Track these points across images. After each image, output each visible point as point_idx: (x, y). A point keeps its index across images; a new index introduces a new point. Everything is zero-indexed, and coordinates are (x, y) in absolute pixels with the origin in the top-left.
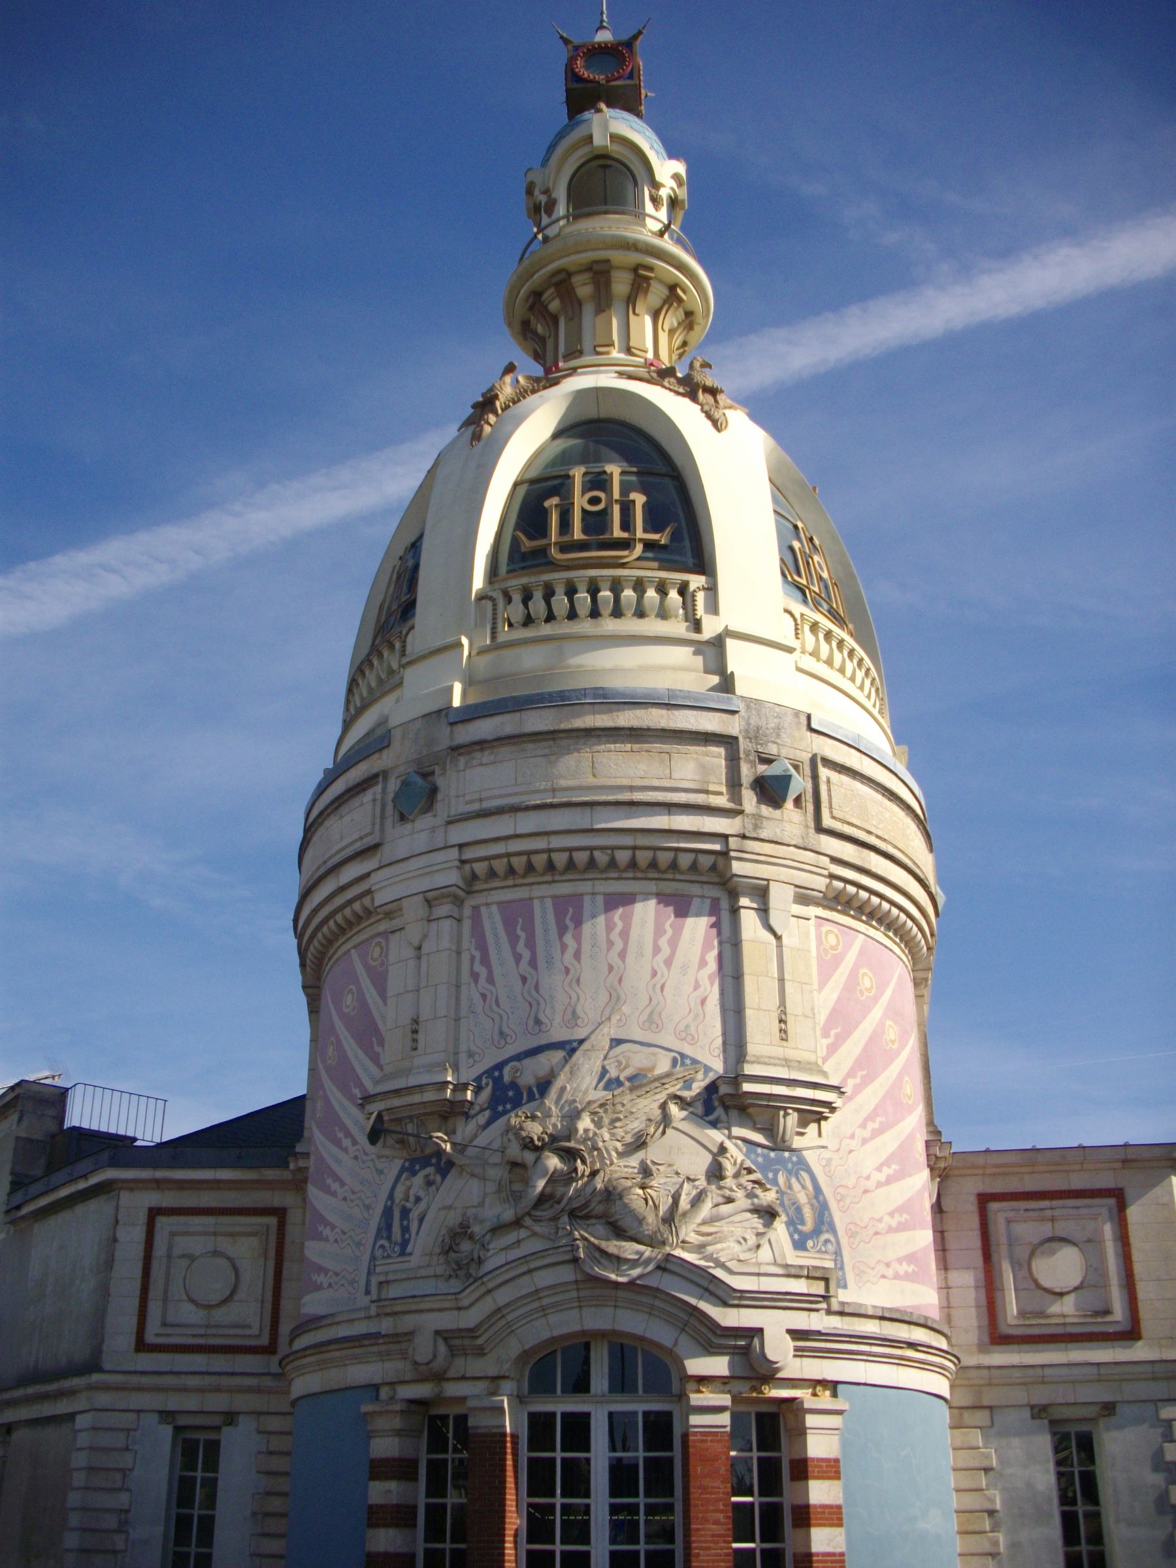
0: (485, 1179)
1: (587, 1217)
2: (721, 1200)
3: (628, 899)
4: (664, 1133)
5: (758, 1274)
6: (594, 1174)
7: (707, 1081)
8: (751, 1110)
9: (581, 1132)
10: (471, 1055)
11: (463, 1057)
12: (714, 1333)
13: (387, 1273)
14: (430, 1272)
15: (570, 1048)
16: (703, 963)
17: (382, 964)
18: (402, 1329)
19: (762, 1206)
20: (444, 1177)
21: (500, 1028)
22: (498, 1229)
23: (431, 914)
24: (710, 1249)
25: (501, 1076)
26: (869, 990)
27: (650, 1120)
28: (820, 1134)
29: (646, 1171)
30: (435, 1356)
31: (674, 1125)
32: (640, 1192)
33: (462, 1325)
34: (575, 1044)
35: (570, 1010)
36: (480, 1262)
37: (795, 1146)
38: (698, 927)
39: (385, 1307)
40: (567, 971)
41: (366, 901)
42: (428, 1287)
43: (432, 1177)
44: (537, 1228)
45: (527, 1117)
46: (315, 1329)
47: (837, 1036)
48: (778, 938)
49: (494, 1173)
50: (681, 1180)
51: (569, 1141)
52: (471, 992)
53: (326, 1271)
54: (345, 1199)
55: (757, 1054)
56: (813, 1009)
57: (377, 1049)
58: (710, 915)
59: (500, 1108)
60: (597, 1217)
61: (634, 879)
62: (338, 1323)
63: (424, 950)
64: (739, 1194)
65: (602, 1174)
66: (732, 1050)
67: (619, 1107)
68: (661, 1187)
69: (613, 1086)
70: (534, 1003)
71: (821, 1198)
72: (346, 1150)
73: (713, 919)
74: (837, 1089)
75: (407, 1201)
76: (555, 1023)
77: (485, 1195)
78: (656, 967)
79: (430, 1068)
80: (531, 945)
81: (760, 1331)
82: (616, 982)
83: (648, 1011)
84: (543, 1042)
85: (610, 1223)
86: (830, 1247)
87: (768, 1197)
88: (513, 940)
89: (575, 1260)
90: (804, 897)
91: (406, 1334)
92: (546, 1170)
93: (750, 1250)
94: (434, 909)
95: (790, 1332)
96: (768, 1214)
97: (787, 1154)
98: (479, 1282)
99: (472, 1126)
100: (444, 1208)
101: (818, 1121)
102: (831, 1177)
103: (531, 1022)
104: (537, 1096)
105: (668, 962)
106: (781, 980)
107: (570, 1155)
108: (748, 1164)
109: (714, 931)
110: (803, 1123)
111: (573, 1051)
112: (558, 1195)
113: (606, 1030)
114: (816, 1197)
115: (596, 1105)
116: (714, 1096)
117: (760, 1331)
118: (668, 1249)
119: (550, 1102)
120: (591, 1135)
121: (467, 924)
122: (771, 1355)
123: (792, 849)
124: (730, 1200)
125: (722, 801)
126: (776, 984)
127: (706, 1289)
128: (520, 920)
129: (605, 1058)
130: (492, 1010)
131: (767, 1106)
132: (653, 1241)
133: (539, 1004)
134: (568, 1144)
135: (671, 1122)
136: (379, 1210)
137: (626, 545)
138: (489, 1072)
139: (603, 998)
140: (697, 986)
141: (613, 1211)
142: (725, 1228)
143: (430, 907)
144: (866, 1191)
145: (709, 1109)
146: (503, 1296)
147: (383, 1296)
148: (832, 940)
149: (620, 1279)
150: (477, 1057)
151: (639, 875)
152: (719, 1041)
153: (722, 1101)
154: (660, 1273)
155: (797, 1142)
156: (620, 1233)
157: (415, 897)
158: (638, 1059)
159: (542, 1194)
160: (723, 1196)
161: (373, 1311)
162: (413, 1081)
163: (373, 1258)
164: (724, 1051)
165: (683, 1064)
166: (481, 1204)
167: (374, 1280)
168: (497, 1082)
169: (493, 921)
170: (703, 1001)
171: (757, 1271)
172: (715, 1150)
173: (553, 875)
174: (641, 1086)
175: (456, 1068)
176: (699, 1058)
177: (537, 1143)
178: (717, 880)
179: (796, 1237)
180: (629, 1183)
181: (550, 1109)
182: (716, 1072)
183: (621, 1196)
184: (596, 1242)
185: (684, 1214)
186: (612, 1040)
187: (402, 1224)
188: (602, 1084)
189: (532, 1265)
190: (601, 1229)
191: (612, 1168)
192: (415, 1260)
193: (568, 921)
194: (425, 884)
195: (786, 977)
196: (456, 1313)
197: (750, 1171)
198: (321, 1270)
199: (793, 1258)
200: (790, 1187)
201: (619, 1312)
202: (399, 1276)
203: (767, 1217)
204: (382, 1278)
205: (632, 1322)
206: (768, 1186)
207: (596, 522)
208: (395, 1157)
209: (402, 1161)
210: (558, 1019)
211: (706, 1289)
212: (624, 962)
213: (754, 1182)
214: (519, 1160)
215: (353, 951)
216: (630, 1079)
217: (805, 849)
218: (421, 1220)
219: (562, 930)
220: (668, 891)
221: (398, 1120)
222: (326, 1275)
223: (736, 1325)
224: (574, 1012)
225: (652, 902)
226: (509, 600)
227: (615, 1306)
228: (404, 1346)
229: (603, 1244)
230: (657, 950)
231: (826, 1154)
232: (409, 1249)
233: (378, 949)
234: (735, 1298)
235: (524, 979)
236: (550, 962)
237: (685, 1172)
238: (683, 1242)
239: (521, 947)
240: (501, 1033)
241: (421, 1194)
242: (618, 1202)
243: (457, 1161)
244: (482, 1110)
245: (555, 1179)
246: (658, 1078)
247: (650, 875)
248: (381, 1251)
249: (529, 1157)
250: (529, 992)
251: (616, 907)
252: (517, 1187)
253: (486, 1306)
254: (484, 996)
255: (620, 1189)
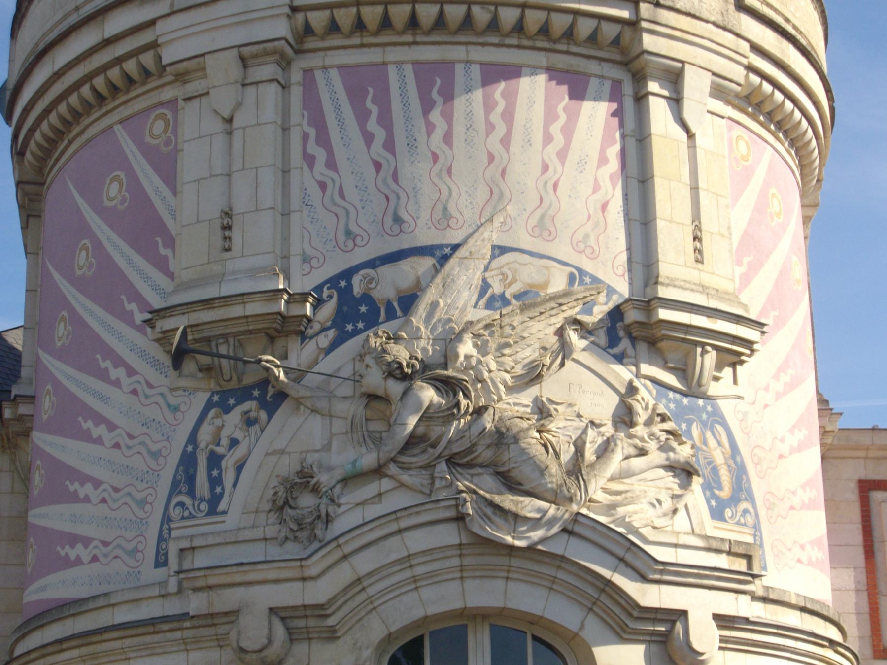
0: (331, 416)
1: (470, 465)
2: (632, 451)
3: (512, 72)
4: (562, 365)
5: (676, 546)
6: (479, 412)
7: (611, 305)
8: (663, 345)
9: (462, 358)
10: (306, 259)
11: (295, 262)
12: (630, 615)
13: (192, 537)
14: (258, 534)
15: (442, 255)
16: (603, 160)
17: (167, 143)
18: (219, 608)
19: (679, 461)
20: (270, 416)
21: (347, 225)
22: (354, 478)
23: (245, 78)
24: (621, 511)
25: (350, 286)
26: (778, 214)
27: (544, 348)
28: (735, 382)
29: (542, 411)
30: (270, 641)
31: (574, 356)
32: (537, 435)
33: (309, 601)
34: (447, 251)
35: (439, 207)
36: (329, 520)
37: (710, 392)
38: (596, 114)
39: (188, 581)
40: (435, 158)
41: (147, 59)
42: (256, 552)
43: (253, 415)
44: (405, 478)
45: (389, 338)
46: (73, 615)
47: (749, 264)
48: (691, 135)
49: (349, 408)
50: (583, 424)
51: (446, 368)
52: (303, 180)
53: (86, 541)
54: (117, 446)
55: (671, 276)
56: (729, 228)
57: (163, 251)
58: (611, 100)
59: (350, 327)
60: (482, 466)
61: (519, 47)
62: (114, 605)
63: (236, 123)
64: (652, 446)
65: (491, 411)
66: (638, 269)
67: (508, 330)
68: (563, 431)
69: (498, 305)
70: (392, 197)
71: (738, 459)
72: (117, 383)
73: (615, 106)
74: (758, 325)
75: (218, 445)
76: (419, 222)
77: (332, 435)
78: (547, 160)
79: (253, 273)
81: (684, 613)
82: (498, 176)
83: (539, 213)
84: (406, 246)
85: (498, 474)
86: (750, 520)
87: (684, 452)
88: (362, 116)
89: (460, 518)
90: (718, 92)
91: (226, 614)
92: (420, 403)
93: (665, 515)
94: (251, 71)
95: (717, 617)
96: (685, 472)
97: (701, 402)
98: (334, 544)
99: (310, 348)
100: (274, 452)
101: (733, 365)
102: (747, 434)
103: (389, 220)
104: (399, 313)
105: (562, 155)
106: (695, 189)
107: (449, 386)
108: (661, 409)
109: (616, 120)
110: (719, 367)
111: (445, 258)
112: (433, 436)
113: (487, 235)
114: (733, 457)
115: (481, 325)
116: (619, 324)
117: (684, 613)
118: (574, 508)
119: (418, 319)
120: (474, 362)
121: (296, 92)
122: (697, 645)
123: (710, 26)
124: (642, 452)
126: (687, 193)
127: (622, 560)
128: (371, 90)
129: (486, 269)
130: (335, 204)
131: (684, 340)
132: (557, 497)
133: (398, 198)
134: (446, 372)
135: (571, 352)
138: (333, 282)
139: (482, 194)
140: (596, 188)
141: (505, 457)
142: (636, 487)
143: (245, 67)
144: (781, 456)
145: (613, 341)
146: (364, 563)
147: (186, 566)
148: (742, 148)
149: (519, 543)
150: (314, 262)
151: (526, 43)
152: (624, 257)
153: (628, 330)
154: (565, 536)
155: (713, 389)
156: (512, 485)
157: (226, 53)
158: (528, 273)
159: (412, 435)
160: (635, 447)
161: (173, 586)
162: (227, 289)
163: (166, 519)
164: (630, 270)
165: (581, 282)
166: (327, 448)
167: (172, 549)
168: (345, 294)
169: (332, 91)
170: (604, 207)
171: (674, 541)
172: (623, 390)
173: (414, 35)
174: (534, 305)
175: (287, 278)
176: (600, 276)
177: (406, 370)
178: (618, 57)
179: (713, 503)
180: (525, 424)
181: (418, 328)
182: (621, 295)
183: (516, 440)
184: (488, 495)
185: (592, 466)
186: (494, 247)
187: (210, 475)
188: (483, 302)
189: (404, 524)
190: (489, 480)
191: (499, 405)
192: (232, 520)
193: (434, 94)
194: (240, 36)
195: (701, 184)
196: (299, 584)
197: (664, 418)
198: (73, 540)
199: (713, 529)
200: (705, 442)
201: (511, 584)
202: (211, 540)
203: (684, 475)
204: (185, 544)
205: (527, 598)
206: (685, 440)
208: (197, 390)
209: (208, 394)
210: (425, 216)
211: (622, 560)
212: (507, 149)
213: (668, 432)
214: (380, 392)
215: (118, 128)
216: (517, 297)
217: (725, 29)
218: (239, 469)
219: (427, 106)
220: (560, 66)
221: (208, 340)
222: (86, 547)
223: (657, 605)
224: (445, 209)
225: (542, 79)
227: (507, 578)
228: (222, 630)
229: (497, 499)
230: (548, 139)
231: (742, 405)
232: (222, 506)
233: (159, 126)
234: (656, 571)
235: (378, 166)
236: (412, 145)
237: (589, 413)
238: (591, 501)
239: (372, 125)
240: (348, 233)
241: (239, 435)
242: (512, 446)
243: (292, 393)
244: (324, 329)
245: (428, 416)
246: (554, 298)
247: (539, 44)
248: (179, 510)
249: (395, 388)
250: (385, 181)
251: (497, 81)
252: (375, 426)
253: (343, 575)
254: (323, 186)
255: (515, 430)
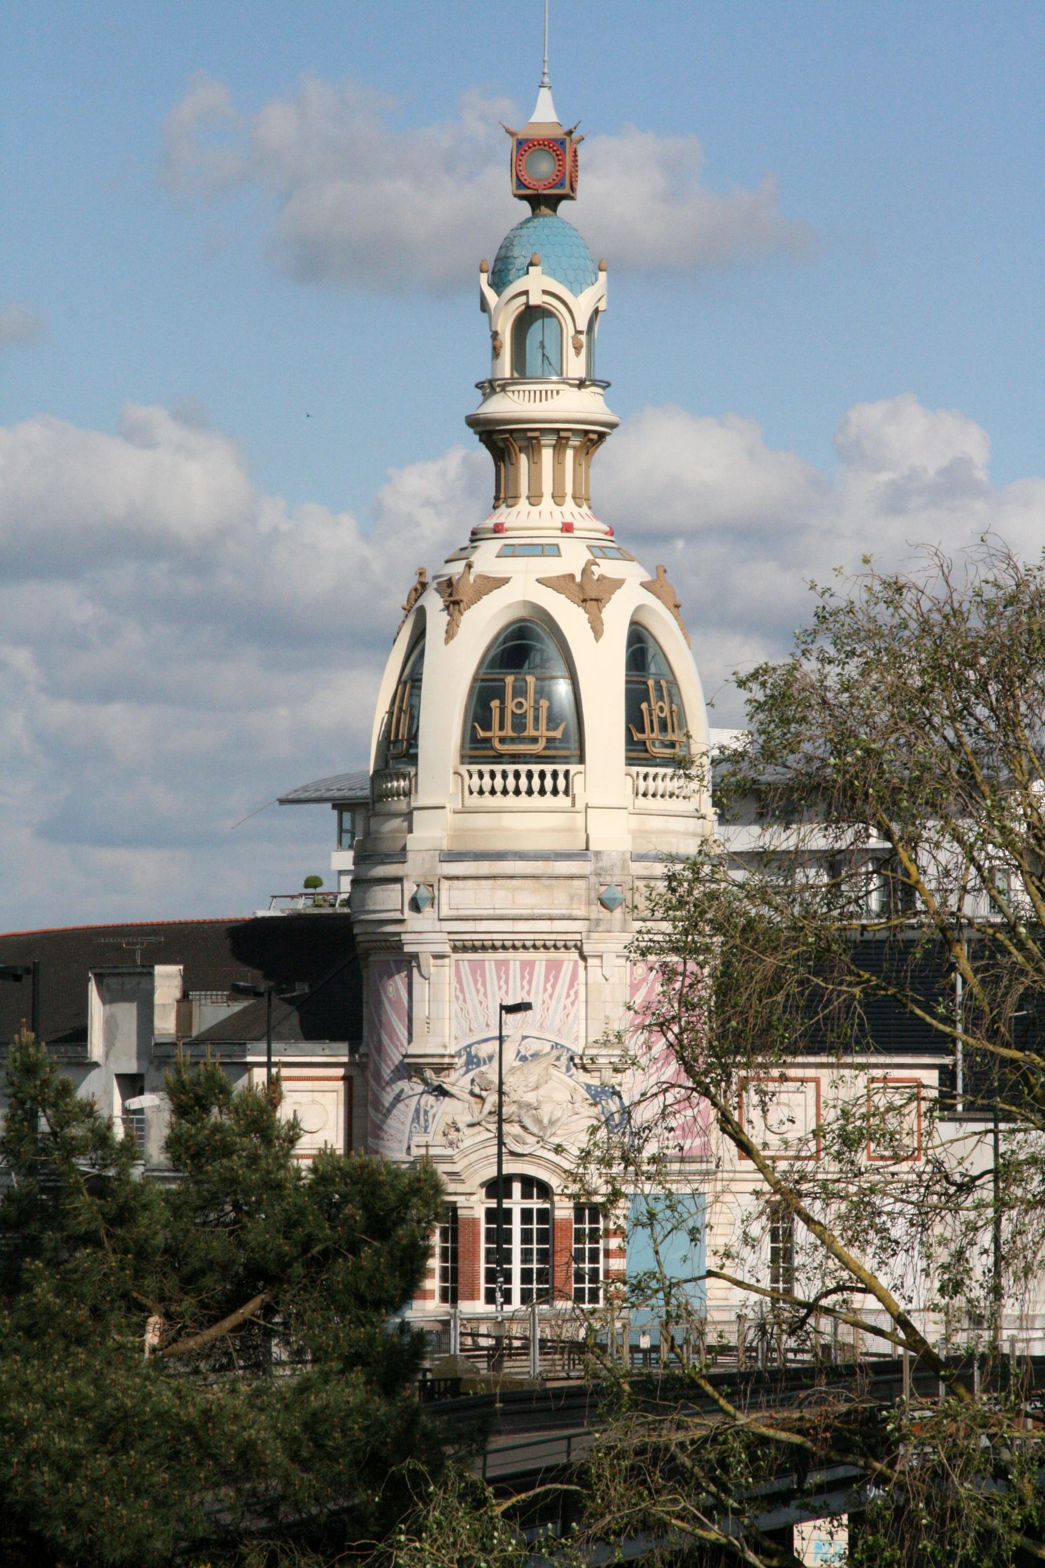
80: (484, 984)
88: (476, 981)
125: (581, 912)
136: (413, 1108)
137: (534, 740)
138: (465, 1048)
146: (473, 1157)
158: (534, 1046)
168: (469, 1054)
207: (519, 723)
226: (471, 776)
239: (479, 986)
